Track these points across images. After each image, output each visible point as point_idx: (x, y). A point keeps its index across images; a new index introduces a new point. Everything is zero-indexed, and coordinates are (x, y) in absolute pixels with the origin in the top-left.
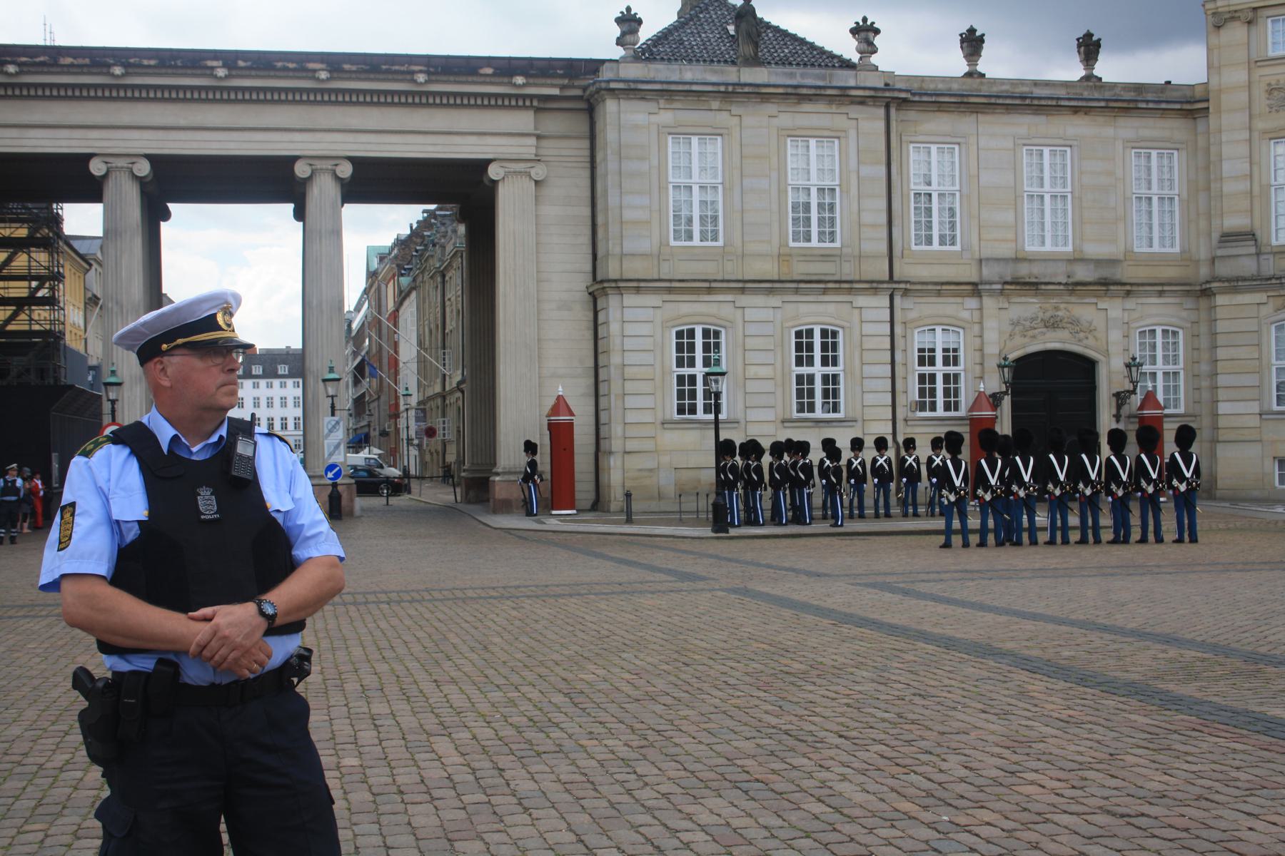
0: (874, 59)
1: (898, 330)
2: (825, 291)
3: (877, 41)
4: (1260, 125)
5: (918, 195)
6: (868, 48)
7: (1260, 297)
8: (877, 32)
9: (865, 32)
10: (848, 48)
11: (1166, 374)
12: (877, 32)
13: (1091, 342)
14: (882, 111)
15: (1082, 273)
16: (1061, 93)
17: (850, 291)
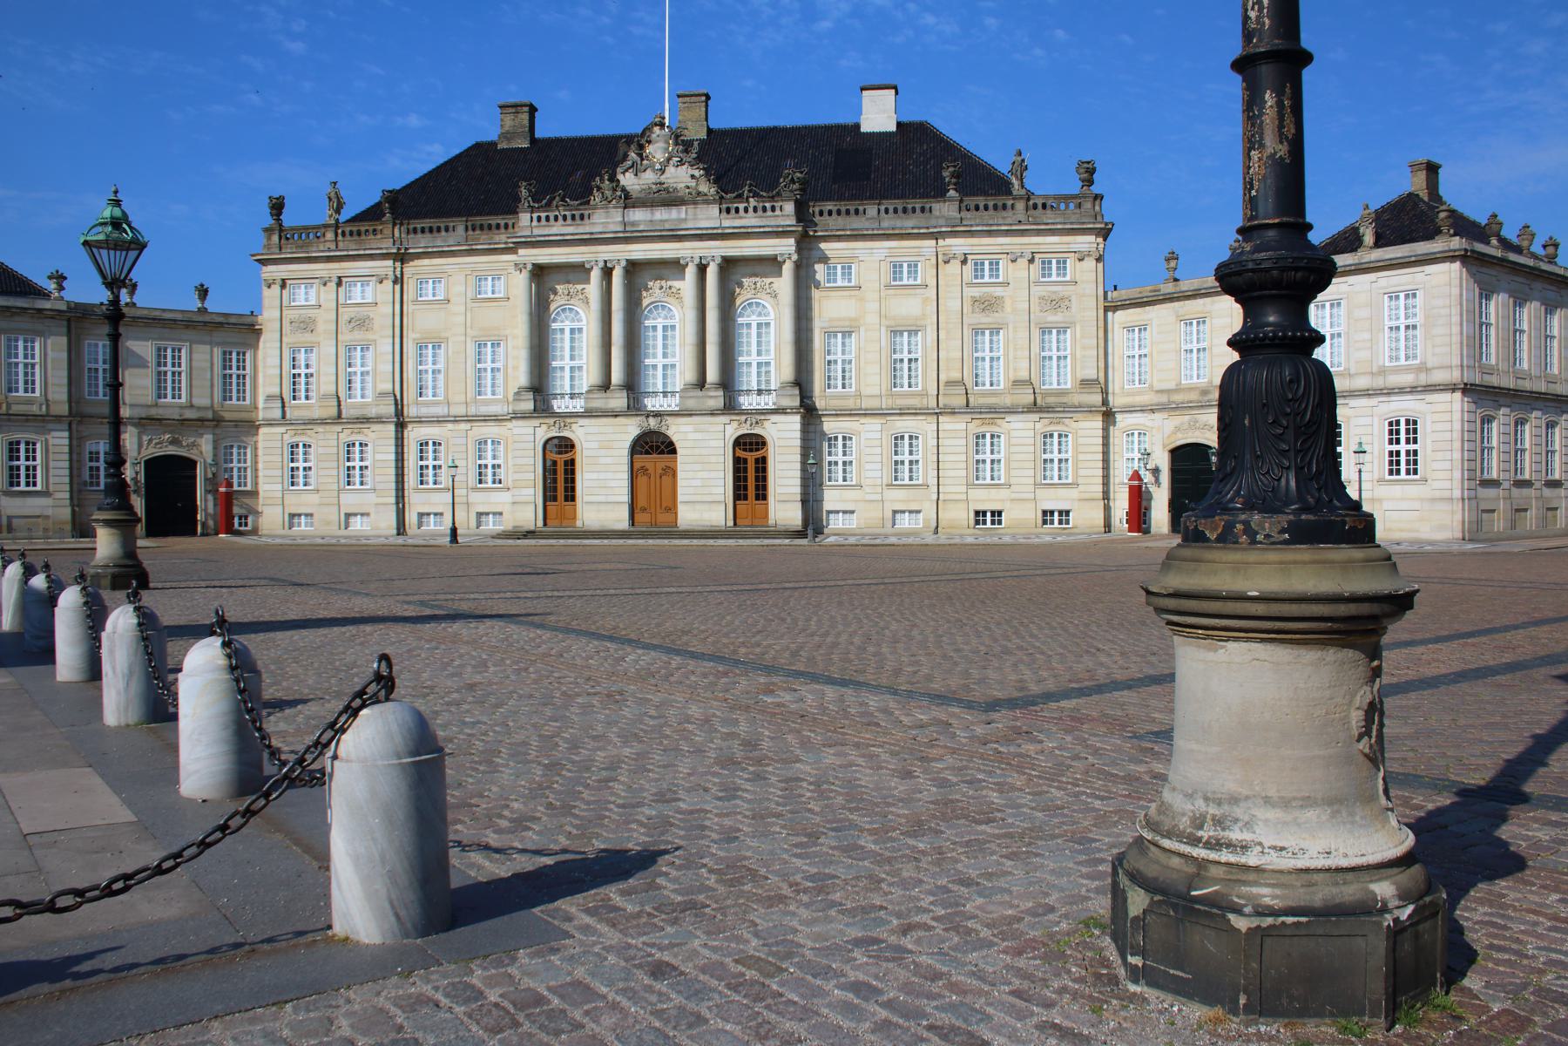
0: (63, 293)
1: (75, 443)
2: (27, 421)
3: (65, 284)
4: (284, 339)
5: (90, 369)
6: (61, 288)
7: (282, 429)
8: (65, 278)
9: (60, 278)
10: (51, 286)
11: (239, 469)
12: (65, 278)
13: (195, 451)
14: (65, 323)
15: (190, 414)
16: (179, 316)
17: (43, 421)
